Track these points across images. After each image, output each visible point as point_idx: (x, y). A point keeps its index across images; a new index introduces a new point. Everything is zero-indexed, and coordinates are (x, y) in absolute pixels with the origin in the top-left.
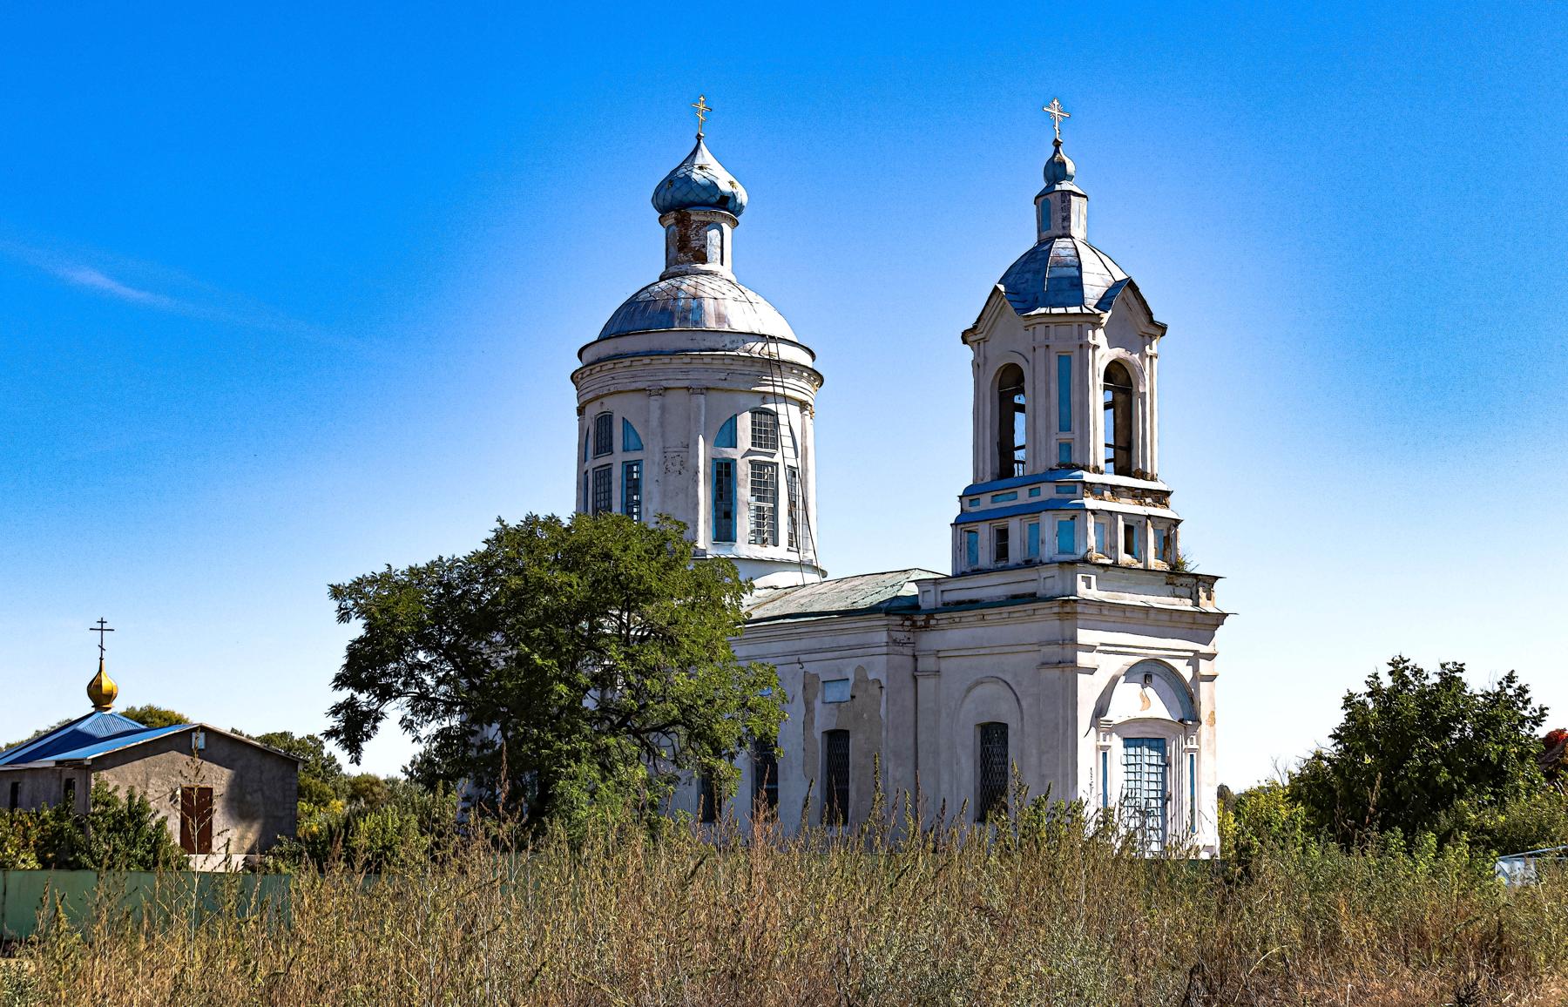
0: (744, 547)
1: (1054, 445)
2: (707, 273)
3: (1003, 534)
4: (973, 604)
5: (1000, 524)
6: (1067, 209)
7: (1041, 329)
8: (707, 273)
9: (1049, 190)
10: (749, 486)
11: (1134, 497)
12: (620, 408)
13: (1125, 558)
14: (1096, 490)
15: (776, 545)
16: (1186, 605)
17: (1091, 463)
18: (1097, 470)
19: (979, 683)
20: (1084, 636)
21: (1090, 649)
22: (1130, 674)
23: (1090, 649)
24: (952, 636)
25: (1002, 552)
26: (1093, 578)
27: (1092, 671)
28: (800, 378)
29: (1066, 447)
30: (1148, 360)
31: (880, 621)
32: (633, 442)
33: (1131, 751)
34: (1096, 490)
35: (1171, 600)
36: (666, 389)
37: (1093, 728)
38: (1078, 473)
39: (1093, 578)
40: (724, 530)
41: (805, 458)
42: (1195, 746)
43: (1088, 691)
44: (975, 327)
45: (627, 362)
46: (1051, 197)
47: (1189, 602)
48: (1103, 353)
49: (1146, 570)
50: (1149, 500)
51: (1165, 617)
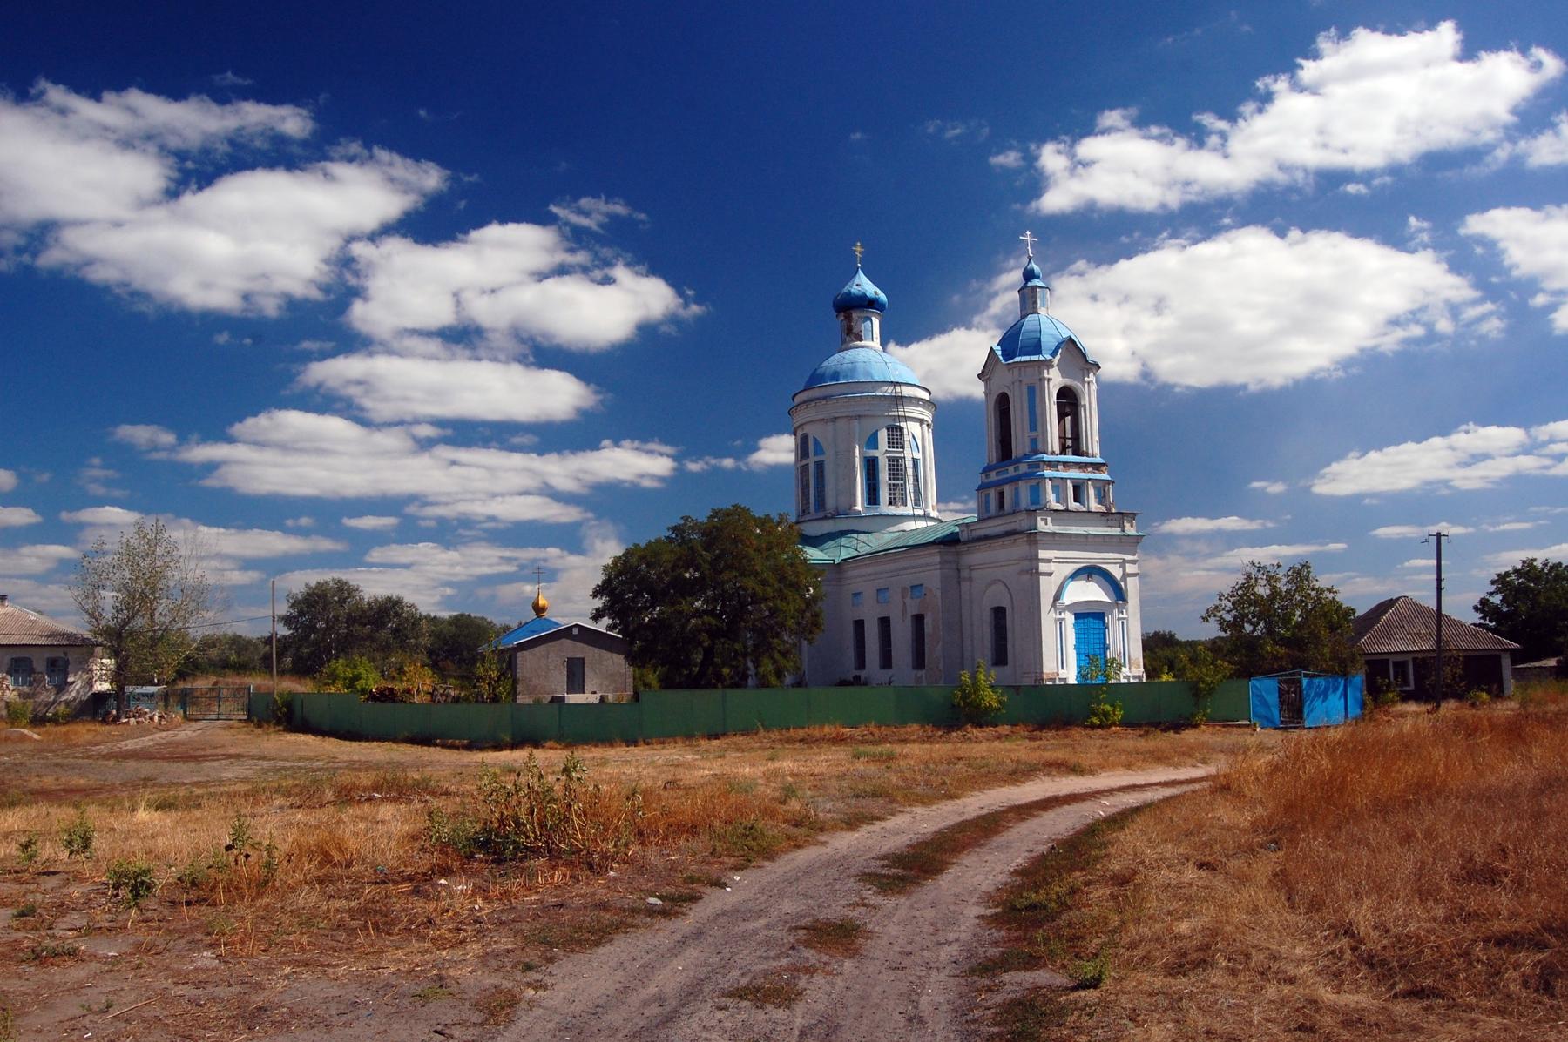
0: (885, 508)
1: (1027, 441)
2: (863, 347)
3: (1001, 495)
4: (986, 538)
5: (999, 488)
6: (1035, 297)
7: (1016, 371)
8: (863, 347)
9: (1024, 287)
10: (887, 472)
11: (1080, 468)
12: (812, 431)
13: (1073, 505)
14: (1053, 465)
15: (904, 504)
16: (1116, 531)
17: (1050, 449)
18: (1053, 453)
19: (990, 585)
20: (1043, 554)
21: (1049, 561)
22: (1075, 575)
23: (1049, 561)
24: (977, 556)
25: (1001, 505)
26: (1049, 519)
27: (1050, 574)
28: (918, 405)
29: (1034, 441)
30: (1086, 385)
31: (934, 550)
32: (819, 449)
33: (1081, 621)
34: (1053, 465)
35: (1106, 528)
36: (836, 418)
37: (368, 559)
38: (1040, 456)
39: (1049, 519)
40: (873, 498)
41: (924, 453)
42: (1125, 616)
43: (1047, 587)
44: (983, 372)
45: (813, 404)
46: (1026, 290)
47: (1119, 529)
48: (1055, 379)
49: (1067, 510)
50: (1090, 469)
51: (1100, 539)
